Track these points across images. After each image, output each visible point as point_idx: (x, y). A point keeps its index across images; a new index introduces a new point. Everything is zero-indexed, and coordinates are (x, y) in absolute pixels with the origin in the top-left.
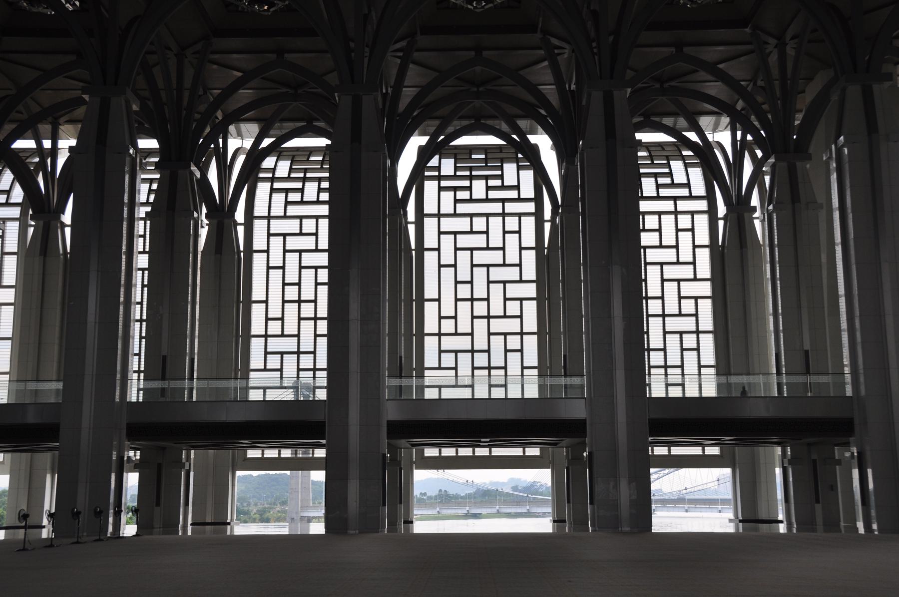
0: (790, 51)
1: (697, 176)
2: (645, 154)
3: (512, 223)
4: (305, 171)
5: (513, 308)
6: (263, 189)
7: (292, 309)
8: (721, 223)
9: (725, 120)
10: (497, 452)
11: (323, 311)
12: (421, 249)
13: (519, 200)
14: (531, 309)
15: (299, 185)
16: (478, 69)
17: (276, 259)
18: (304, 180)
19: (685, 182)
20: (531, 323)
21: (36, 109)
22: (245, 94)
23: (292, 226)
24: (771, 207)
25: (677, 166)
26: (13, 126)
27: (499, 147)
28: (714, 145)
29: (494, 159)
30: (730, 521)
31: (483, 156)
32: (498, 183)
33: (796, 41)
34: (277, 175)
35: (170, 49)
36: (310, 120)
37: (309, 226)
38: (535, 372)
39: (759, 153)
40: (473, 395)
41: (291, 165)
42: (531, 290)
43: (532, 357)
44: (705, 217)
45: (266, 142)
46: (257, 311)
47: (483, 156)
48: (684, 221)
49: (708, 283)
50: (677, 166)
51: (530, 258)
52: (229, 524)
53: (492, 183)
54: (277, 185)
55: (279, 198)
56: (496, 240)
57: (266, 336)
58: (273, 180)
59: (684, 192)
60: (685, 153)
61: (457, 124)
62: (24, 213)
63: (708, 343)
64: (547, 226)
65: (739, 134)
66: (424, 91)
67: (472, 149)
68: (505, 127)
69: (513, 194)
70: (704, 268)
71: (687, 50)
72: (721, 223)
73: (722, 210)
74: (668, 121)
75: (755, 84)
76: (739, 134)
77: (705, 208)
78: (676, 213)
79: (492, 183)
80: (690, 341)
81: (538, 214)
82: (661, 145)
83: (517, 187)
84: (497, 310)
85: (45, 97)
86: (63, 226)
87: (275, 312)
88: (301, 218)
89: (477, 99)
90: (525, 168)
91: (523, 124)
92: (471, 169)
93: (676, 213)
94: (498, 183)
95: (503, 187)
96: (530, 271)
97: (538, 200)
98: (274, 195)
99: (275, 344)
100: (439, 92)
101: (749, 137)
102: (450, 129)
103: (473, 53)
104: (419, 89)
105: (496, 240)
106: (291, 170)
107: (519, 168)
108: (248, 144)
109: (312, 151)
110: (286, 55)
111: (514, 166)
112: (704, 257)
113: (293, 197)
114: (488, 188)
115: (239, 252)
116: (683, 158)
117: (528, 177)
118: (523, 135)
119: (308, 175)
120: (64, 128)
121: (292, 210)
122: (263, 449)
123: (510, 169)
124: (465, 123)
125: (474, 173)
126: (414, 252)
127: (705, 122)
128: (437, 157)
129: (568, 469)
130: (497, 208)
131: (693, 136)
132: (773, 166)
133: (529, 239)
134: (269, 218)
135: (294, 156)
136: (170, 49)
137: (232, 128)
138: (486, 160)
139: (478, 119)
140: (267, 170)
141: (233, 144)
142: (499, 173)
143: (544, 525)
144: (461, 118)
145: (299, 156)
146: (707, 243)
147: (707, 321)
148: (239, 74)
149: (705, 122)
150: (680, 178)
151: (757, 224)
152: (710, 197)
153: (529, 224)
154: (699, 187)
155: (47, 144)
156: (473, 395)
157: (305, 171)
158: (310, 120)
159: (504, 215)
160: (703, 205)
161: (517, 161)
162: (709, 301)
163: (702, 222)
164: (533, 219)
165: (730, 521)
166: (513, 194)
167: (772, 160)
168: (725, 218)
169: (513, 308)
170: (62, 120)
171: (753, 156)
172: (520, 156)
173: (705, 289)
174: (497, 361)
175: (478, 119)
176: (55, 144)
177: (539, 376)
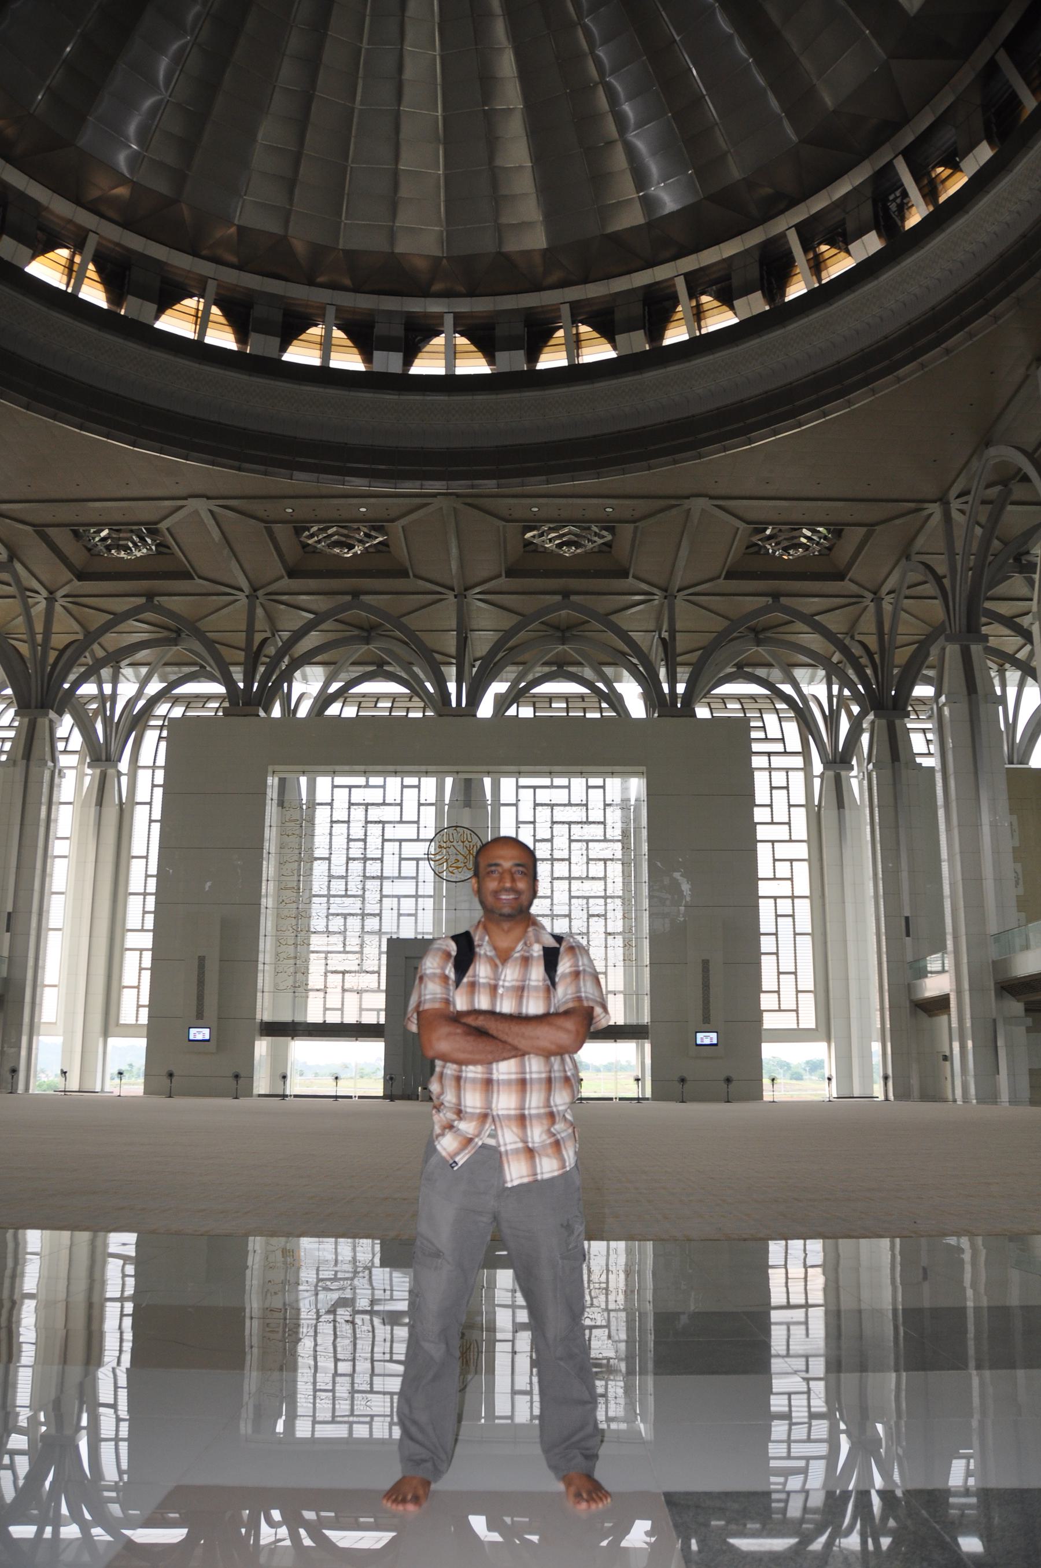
0: (887, 607)
1: (792, 730)
2: (739, 706)
7: (356, 867)
8: (817, 782)
9: (821, 673)
12: (497, 804)
16: (563, 612)
19: (780, 737)
21: (100, 653)
22: (312, 640)
24: (870, 766)
25: (771, 719)
26: (82, 669)
27: (582, 697)
28: (810, 698)
33: (892, 595)
35: (242, 591)
39: (856, 709)
44: (801, 774)
45: (335, 687)
46: (319, 869)
47: (564, 705)
48: (779, 779)
49: (805, 845)
50: (771, 719)
59: (779, 747)
60: (778, 706)
61: (539, 671)
62: (81, 762)
63: (804, 908)
65: (835, 689)
66: (508, 634)
67: (551, 698)
68: (588, 673)
70: (800, 830)
71: (783, 600)
72: (817, 782)
73: (818, 767)
74: (761, 672)
75: (852, 638)
76: (835, 689)
77: (802, 766)
78: (770, 769)
80: (784, 906)
82: (753, 698)
85: (112, 640)
86: (119, 774)
87: (339, 870)
91: (609, 671)
93: (770, 769)
100: (522, 635)
101: (846, 692)
102: (530, 677)
104: (501, 634)
108: (314, 688)
109: (378, 697)
110: (362, 597)
112: (800, 816)
116: (777, 711)
118: (609, 683)
120: (127, 671)
124: (547, 669)
126: (489, 807)
127: (799, 673)
128: (515, 705)
131: (787, 689)
132: (873, 723)
135: (360, 703)
136: (242, 591)
137: (298, 674)
138: (567, 709)
139: (560, 666)
141: (298, 688)
144: (545, 664)
146: (803, 802)
147: (803, 886)
148: (312, 616)
149: (799, 673)
150: (773, 731)
151: (855, 783)
152: (805, 753)
154: (794, 742)
155: (107, 689)
158: (381, 664)
160: (798, 762)
162: (806, 864)
163: (797, 780)
167: (871, 717)
168: (822, 776)
170: (123, 664)
171: (849, 713)
172: (604, 705)
173: (802, 851)
175: (560, 666)
176: (114, 689)
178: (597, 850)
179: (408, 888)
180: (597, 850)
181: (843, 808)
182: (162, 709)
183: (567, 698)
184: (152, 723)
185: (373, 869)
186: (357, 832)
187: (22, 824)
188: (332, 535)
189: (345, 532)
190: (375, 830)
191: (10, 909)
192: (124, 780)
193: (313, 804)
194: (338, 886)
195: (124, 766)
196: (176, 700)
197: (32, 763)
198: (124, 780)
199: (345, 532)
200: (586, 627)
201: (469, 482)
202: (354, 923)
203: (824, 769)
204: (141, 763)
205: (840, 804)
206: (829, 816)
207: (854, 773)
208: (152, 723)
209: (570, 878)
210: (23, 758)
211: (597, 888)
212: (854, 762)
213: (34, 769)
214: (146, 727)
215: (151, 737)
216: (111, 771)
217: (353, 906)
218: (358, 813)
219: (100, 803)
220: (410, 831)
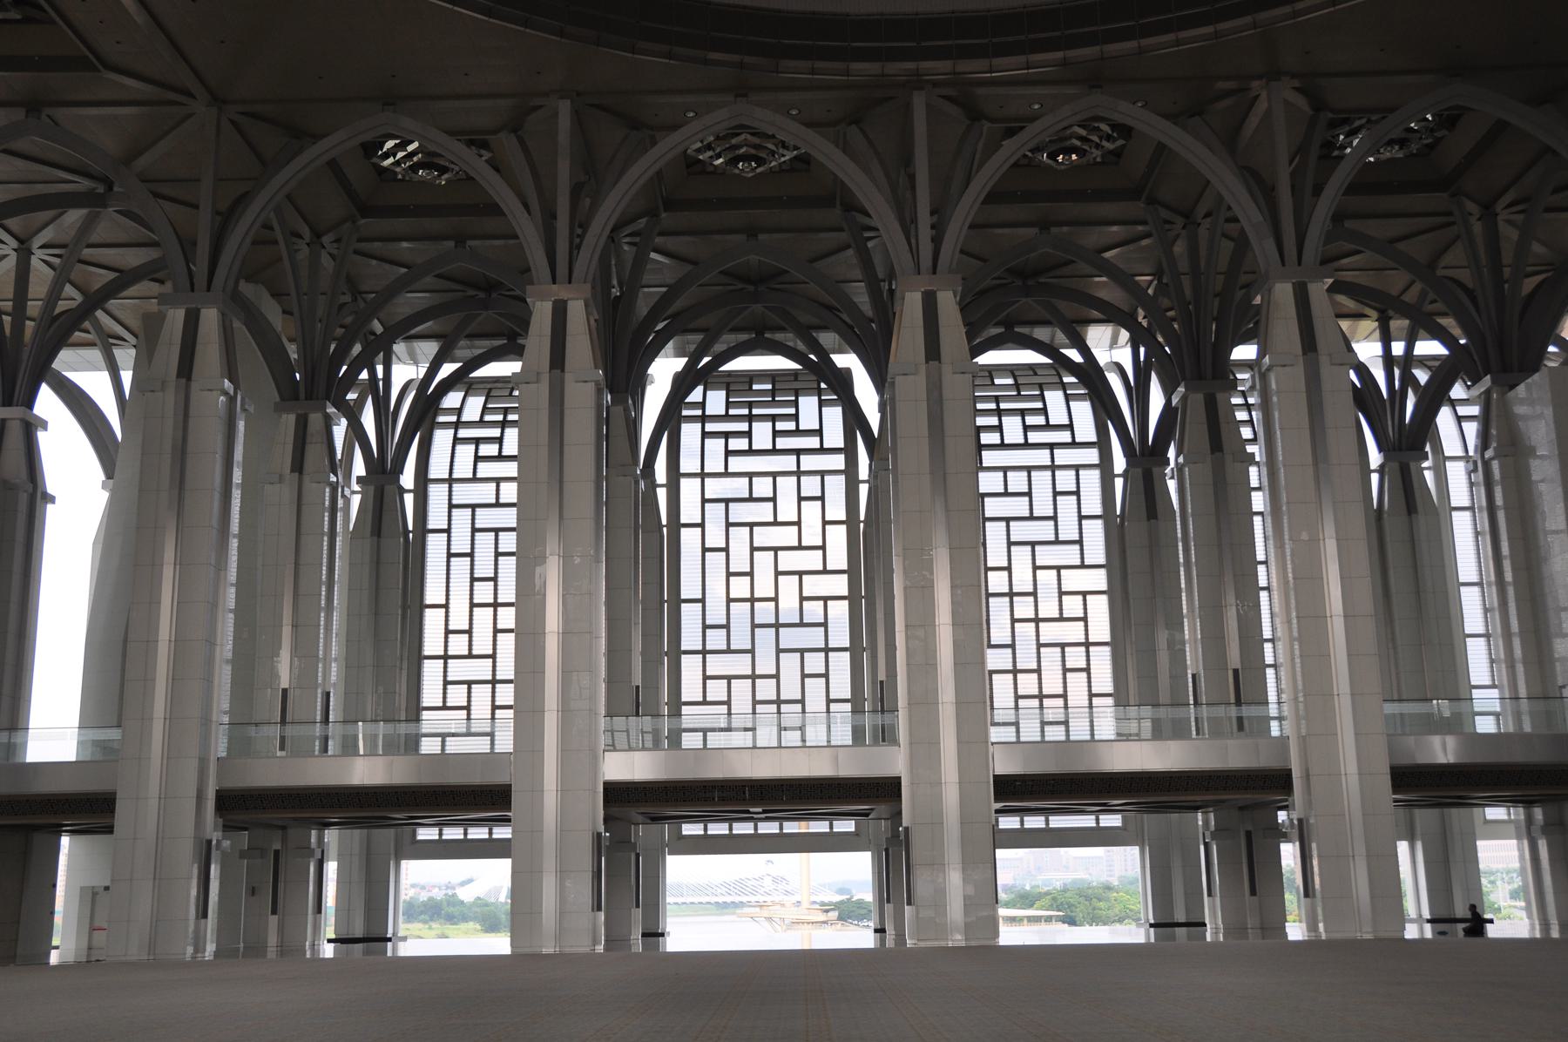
3: (1066, 480)
4: (750, 405)
5: (1073, 606)
6: (690, 433)
9: (1369, 325)
10: (1057, 822)
11: (998, 608)
13: (1074, 444)
14: (1100, 608)
15: (744, 427)
17: (715, 538)
18: (750, 418)
20: (1101, 628)
23: (738, 487)
27: (1032, 368)
29: (1030, 385)
30: (1491, 921)
31: (1010, 381)
32: (1040, 420)
34: (708, 413)
36: (1009, 324)
37: (763, 487)
38: (1110, 701)
40: (1068, 735)
41: (728, 397)
42: (1099, 580)
43: (1103, 678)
46: (690, 614)
51: (1095, 534)
52: (1151, 925)
53: (1030, 420)
54: (710, 427)
55: (715, 447)
56: (1043, 506)
57: (827, 650)
58: (704, 419)
64: (1119, 483)
69: (1065, 437)
79: (1030, 420)
81: (1105, 464)
83: (1070, 427)
84: (1048, 608)
86: (402, 491)
88: (751, 475)
89: (1025, 295)
90: (1078, 397)
92: (997, 399)
94: (1040, 420)
95: (1048, 427)
96: (1096, 549)
97: (1103, 444)
98: (707, 441)
99: (716, 665)
103: (1035, 230)
105: (1043, 506)
106: (728, 405)
107: (1068, 398)
109: (751, 377)
111: (1059, 394)
113: (735, 444)
114: (1026, 428)
115: (661, 526)
117: (1083, 413)
119: (755, 411)
120: (399, 348)
121: (736, 464)
122: (731, 821)
123: (1054, 398)
125: (1003, 406)
129: (1206, 845)
130: (1042, 457)
133: (1093, 504)
134: (703, 475)
138: (1017, 386)
140: (694, 405)
142: (1039, 405)
143: (1134, 934)
145: (739, 384)
153: (1091, 479)
156: (1068, 735)
157: (750, 405)
158: (760, 333)
159: (1053, 468)
161: (1064, 387)
164: (1096, 473)
165: (1491, 921)
166: (1065, 437)
168: (1381, 470)
169: (1073, 606)
174: (1052, 684)
177: (1117, 705)
178: (1073, 580)
179: (814, 638)
180: (1073, 580)
181: (1416, 512)
182: (452, 399)
183: (1011, 370)
184: (441, 419)
185: (765, 612)
186: (740, 562)
187: (297, 564)
188: (738, 147)
189: (756, 140)
190: (764, 560)
191: (285, 684)
192: (409, 499)
193: (676, 525)
194: (716, 639)
195: (407, 479)
196: (471, 388)
197: (306, 479)
198: (409, 499)
199: (756, 140)
200: (1066, 270)
201: (1022, 59)
202: (741, 689)
203: (1386, 457)
204: (433, 474)
205: (1411, 508)
206: (1394, 527)
207: (1425, 464)
208: (441, 419)
209: (1037, 620)
210: (292, 471)
211: (1074, 632)
212: (1428, 448)
213: (309, 486)
214: (434, 425)
215: (442, 439)
216: (389, 489)
217: (741, 665)
218: (740, 536)
219: (377, 531)
220: (812, 560)
